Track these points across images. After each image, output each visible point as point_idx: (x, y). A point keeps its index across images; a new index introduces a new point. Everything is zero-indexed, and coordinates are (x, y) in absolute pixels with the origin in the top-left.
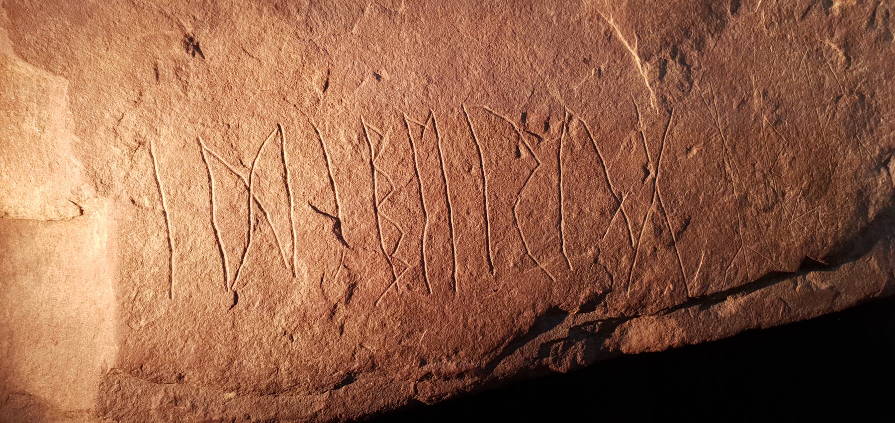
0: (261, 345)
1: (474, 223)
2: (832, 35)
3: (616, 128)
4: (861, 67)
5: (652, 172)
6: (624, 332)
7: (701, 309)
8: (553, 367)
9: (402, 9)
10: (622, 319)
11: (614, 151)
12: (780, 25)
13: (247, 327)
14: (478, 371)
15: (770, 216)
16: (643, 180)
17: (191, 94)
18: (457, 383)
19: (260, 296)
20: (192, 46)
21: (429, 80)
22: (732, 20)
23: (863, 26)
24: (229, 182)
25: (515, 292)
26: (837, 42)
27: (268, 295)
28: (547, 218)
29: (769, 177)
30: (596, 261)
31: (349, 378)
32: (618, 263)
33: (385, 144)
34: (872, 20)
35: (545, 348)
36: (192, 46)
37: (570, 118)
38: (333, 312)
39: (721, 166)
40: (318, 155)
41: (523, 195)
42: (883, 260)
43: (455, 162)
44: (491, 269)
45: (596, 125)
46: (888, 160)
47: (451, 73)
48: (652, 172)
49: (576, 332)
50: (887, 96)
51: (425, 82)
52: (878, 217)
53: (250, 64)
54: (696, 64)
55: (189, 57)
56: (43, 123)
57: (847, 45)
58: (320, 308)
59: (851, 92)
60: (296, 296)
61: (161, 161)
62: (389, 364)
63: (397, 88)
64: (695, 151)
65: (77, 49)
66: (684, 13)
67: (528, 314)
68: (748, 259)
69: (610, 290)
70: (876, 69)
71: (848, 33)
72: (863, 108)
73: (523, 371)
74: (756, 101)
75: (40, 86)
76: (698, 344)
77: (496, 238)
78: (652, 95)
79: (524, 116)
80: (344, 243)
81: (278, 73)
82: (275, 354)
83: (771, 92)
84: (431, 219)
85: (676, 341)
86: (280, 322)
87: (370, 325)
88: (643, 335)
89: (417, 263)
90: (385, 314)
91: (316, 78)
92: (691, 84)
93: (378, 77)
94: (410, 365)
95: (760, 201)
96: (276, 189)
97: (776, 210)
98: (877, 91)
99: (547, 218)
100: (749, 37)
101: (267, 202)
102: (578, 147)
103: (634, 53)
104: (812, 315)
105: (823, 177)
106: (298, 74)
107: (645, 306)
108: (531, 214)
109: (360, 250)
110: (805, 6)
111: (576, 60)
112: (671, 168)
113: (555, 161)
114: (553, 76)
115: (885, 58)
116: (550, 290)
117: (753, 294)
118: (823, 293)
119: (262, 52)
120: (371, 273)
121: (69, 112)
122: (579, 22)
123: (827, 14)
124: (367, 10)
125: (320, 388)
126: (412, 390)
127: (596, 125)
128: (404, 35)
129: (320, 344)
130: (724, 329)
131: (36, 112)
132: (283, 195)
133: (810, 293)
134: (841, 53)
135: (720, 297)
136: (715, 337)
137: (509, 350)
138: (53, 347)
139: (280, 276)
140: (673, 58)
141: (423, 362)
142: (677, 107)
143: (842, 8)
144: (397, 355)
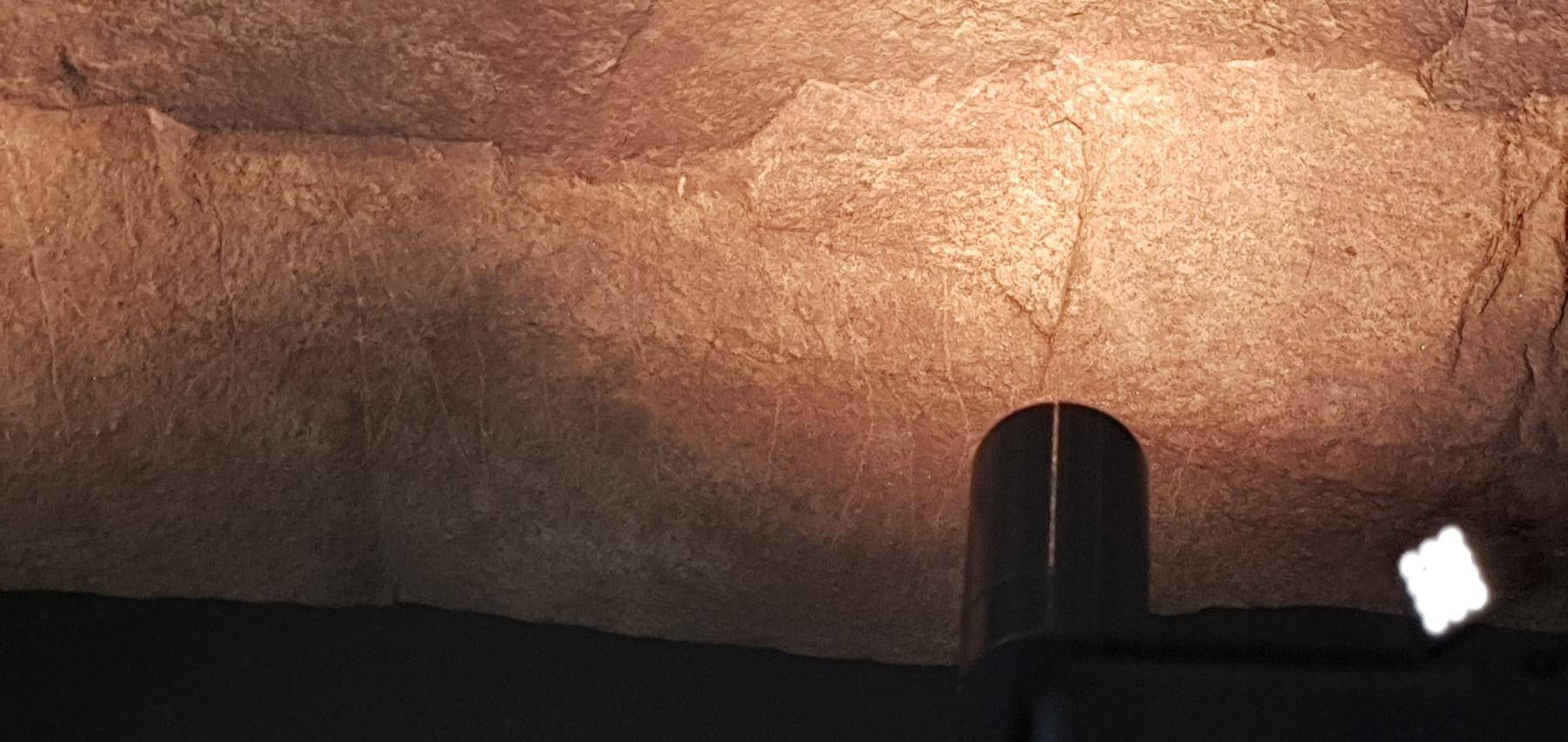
56: (881, 149)
65: (748, 63)
75: (803, 146)
121: (874, 85)
131: (856, 158)
138: (1358, 261)
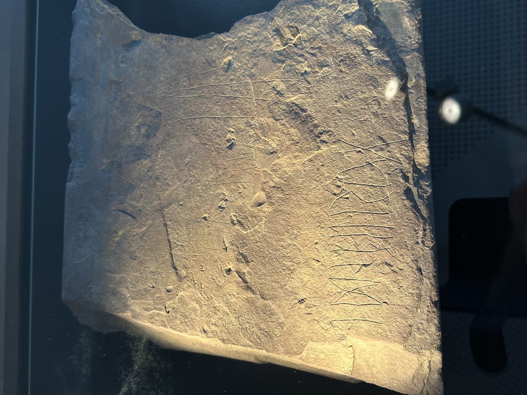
0: (402, 297)
1: (369, 217)
2: (317, 72)
3: (342, 162)
4: (330, 60)
5: (360, 149)
6: (420, 164)
7: (415, 134)
8: (428, 195)
9: (296, 232)
10: (414, 166)
11: (350, 163)
12: (311, 93)
13: (395, 301)
14: (424, 224)
15: (382, 103)
16: (362, 153)
17: (317, 304)
18: (428, 232)
19: (386, 295)
20: (302, 301)
21: (319, 226)
22: (309, 112)
23: (315, 59)
24: (346, 298)
25: (397, 206)
26: (320, 70)
27: (385, 292)
28: (371, 190)
29: (367, 103)
30: (389, 174)
31: (420, 270)
32: (392, 166)
33: (338, 245)
34: (313, 55)
35: (420, 197)
36: (302, 301)
37: (337, 178)
38: (394, 271)
39: (361, 122)
40: (340, 267)
41: (362, 198)
42: (407, 53)
43: (348, 221)
44: (387, 213)
45: (340, 169)
46: (367, 50)
47: (317, 219)
48: (360, 149)
49: (416, 184)
50: (342, 50)
51: (319, 228)
52: (389, 56)
53: (309, 284)
54: (323, 128)
55: (305, 303)
57: (322, 66)
58: (392, 275)
59: (339, 65)
60: (387, 283)
61: (337, 317)
62: (416, 255)
63: (321, 238)
64: (354, 132)
66: (305, 132)
67: (406, 202)
68: (397, 114)
69: (401, 170)
70: (332, 54)
71: (317, 65)
72: (346, 60)
73: (427, 206)
74: (338, 105)
76: (429, 136)
77: (376, 210)
78: (332, 146)
79: (335, 194)
80: (371, 264)
81: (312, 276)
82: (406, 293)
83: (336, 99)
84: (366, 232)
85: (426, 145)
86: (395, 290)
87: (401, 259)
88: (422, 157)
89: (381, 240)
90: (398, 254)
91: (315, 264)
92: (330, 131)
93: (317, 243)
94: (418, 248)
95: (376, 107)
96: (350, 282)
97: (380, 101)
98: (340, 54)
99: (371, 190)
100: (315, 106)
101: (354, 287)
102: (347, 176)
103: (317, 152)
104: (425, 86)
105: (370, 79)
106: (313, 269)
107: (410, 157)
108: (369, 196)
109: (374, 259)
110: (306, 83)
111: (317, 173)
112: (359, 142)
113: (351, 185)
114: (322, 182)
115: (328, 50)
116: (398, 193)
117: (413, 111)
118: (417, 81)
119: (305, 279)
120: (383, 256)
122: (305, 171)
123: (310, 73)
124: (295, 243)
125: (421, 280)
126: (427, 248)
127: (340, 169)
128: (304, 233)
129: (406, 277)
130: (424, 125)
132: (352, 281)
133: (416, 86)
134: (324, 69)
135: (411, 125)
136: (428, 129)
137: (419, 211)
139: (379, 287)
140: (320, 137)
141: (418, 243)
142: (338, 137)
143: (308, 67)
144: (413, 252)
